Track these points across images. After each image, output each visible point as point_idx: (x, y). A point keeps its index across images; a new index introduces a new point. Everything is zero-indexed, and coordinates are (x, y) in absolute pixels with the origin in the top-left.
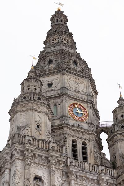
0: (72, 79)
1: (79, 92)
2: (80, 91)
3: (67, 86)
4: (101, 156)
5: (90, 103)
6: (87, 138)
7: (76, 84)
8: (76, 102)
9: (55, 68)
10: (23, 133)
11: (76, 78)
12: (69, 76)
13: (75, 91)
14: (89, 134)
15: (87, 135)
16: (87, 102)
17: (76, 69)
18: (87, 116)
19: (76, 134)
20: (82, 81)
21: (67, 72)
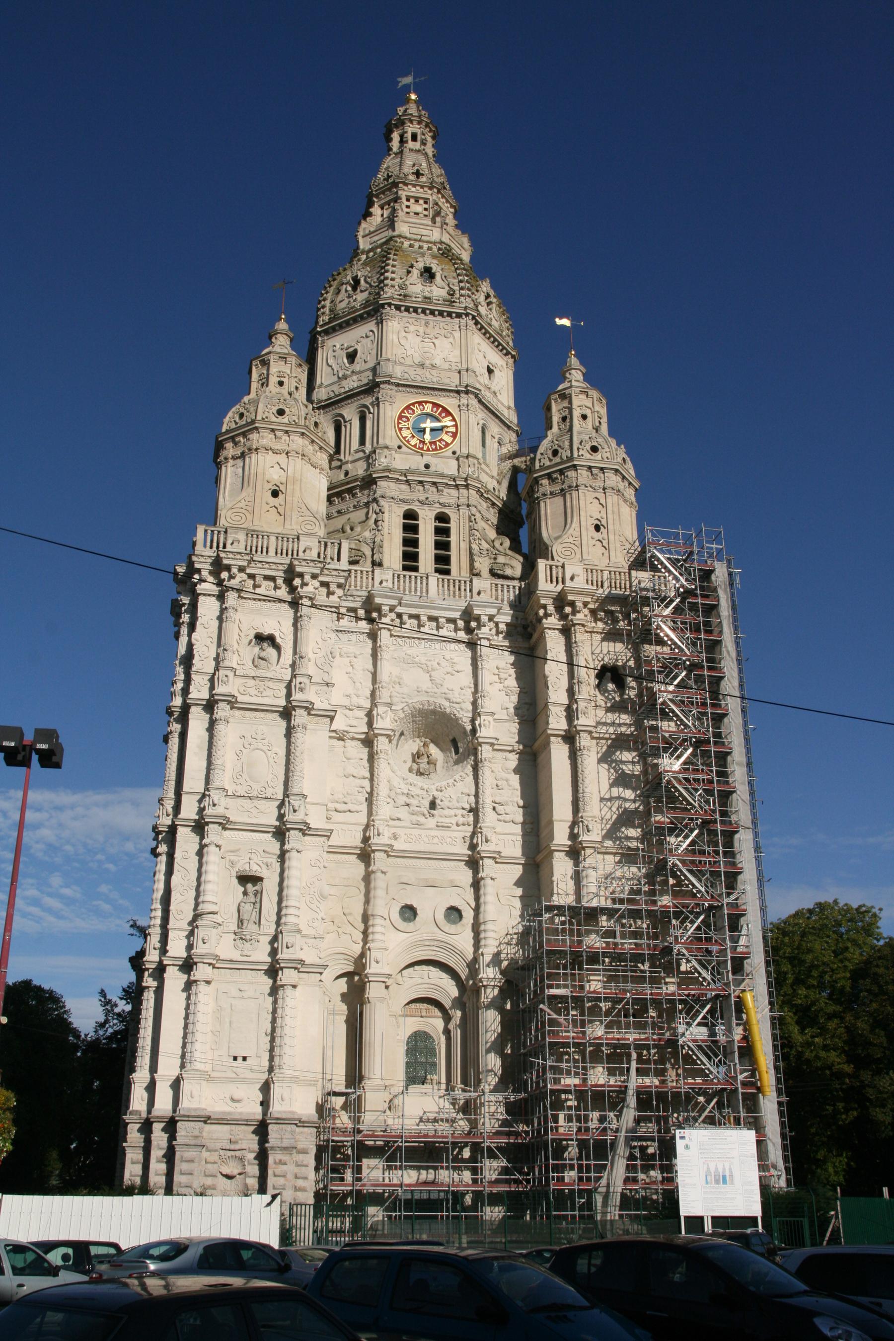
0: (412, 328)
1: (433, 366)
2: (438, 361)
3: (394, 352)
4: (494, 547)
5: (467, 392)
6: (452, 501)
7: (426, 340)
8: (418, 396)
9: (367, 303)
10: (229, 520)
11: (427, 324)
12: (405, 320)
13: (422, 365)
14: (457, 486)
15: (454, 492)
16: (458, 392)
17: (427, 294)
18: (454, 435)
19: (419, 493)
20: (446, 327)
21: (398, 308)
